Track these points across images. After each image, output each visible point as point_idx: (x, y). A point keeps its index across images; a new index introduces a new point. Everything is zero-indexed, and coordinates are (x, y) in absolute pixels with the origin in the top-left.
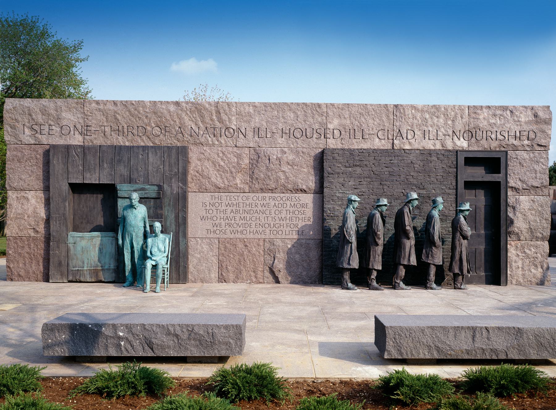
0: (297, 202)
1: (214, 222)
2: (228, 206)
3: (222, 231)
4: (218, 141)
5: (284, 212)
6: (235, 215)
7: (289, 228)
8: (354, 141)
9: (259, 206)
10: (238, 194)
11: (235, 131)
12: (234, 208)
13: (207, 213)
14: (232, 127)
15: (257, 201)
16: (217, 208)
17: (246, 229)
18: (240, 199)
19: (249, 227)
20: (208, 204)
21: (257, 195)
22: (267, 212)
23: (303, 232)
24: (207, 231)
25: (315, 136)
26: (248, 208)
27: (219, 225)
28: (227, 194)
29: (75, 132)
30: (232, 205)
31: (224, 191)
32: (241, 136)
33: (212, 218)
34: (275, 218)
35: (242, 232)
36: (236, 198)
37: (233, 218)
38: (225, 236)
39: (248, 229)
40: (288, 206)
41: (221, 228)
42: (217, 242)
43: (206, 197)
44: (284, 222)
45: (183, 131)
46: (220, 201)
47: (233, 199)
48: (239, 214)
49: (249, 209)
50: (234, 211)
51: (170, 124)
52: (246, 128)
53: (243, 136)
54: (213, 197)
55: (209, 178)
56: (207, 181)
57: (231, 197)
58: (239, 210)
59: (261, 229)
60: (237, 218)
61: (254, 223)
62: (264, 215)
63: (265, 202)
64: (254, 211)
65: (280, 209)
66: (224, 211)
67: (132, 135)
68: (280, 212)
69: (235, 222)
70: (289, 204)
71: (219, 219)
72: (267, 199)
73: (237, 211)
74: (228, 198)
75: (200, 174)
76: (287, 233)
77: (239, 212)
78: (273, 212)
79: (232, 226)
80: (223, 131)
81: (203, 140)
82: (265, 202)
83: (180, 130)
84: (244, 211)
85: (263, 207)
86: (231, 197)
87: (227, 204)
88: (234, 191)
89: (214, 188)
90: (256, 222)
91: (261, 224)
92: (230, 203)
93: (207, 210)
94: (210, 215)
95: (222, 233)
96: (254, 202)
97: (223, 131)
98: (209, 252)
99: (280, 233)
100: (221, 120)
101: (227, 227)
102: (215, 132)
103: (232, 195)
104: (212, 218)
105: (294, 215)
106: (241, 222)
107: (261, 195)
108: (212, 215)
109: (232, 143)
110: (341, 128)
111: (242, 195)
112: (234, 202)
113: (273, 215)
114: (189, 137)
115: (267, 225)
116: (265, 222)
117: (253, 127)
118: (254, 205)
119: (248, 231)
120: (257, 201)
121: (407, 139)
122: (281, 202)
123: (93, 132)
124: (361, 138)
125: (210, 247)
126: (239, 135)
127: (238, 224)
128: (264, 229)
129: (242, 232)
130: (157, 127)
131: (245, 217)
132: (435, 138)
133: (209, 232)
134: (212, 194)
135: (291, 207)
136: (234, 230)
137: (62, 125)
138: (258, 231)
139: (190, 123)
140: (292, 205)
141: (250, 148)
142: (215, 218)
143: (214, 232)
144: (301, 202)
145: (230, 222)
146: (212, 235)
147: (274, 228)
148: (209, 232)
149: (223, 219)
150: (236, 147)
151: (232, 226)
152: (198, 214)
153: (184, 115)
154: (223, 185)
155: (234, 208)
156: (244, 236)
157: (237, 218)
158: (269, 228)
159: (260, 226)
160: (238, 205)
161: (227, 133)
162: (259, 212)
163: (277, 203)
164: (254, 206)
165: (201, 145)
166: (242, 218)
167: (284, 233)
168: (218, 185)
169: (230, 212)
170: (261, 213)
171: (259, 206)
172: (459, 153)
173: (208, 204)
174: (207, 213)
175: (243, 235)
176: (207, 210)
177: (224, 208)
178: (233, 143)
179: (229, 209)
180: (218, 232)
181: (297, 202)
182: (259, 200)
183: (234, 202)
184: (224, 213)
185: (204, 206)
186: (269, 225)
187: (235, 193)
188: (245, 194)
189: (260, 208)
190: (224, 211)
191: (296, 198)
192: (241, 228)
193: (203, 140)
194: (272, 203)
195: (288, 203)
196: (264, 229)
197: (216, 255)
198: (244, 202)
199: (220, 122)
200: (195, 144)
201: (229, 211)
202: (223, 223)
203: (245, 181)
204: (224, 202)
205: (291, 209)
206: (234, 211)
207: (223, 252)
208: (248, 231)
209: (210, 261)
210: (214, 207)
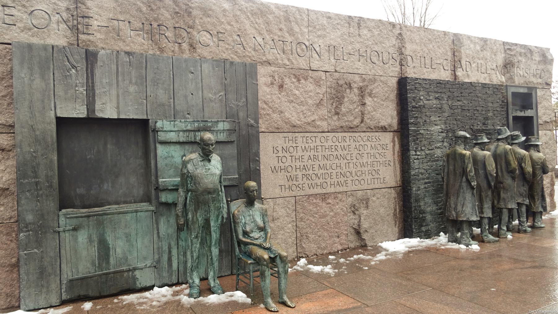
0: (377, 143)
1: (288, 175)
2: (305, 151)
3: (299, 186)
4: (289, 60)
5: (366, 155)
6: (313, 163)
7: (371, 176)
8: (425, 70)
9: (339, 150)
10: (315, 134)
11: (308, 48)
12: (312, 153)
13: (280, 161)
14: (305, 42)
15: (337, 143)
16: (292, 154)
17: (326, 181)
18: (318, 140)
19: (329, 179)
20: (280, 149)
21: (337, 135)
22: (348, 157)
23: (385, 179)
24: (280, 188)
25: (391, 62)
26: (328, 153)
27: (295, 179)
28: (302, 134)
29: (60, 24)
30: (309, 150)
31: (300, 130)
32: (315, 55)
33: (286, 169)
34: (357, 164)
35: (321, 186)
36: (313, 139)
37: (311, 168)
38: (303, 193)
39: (328, 180)
40: (369, 148)
41: (298, 182)
42: (293, 201)
43: (279, 141)
44: (366, 169)
45: (243, 42)
46: (294, 145)
47: (310, 141)
48: (317, 161)
49: (329, 153)
50: (312, 157)
51: (226, 30)
52: (320, 46)
53: (317, 56)
54: (287, 139)
55: (282, 112)
56: (278, 116)
57: (307, 139)
58: (317, 156)
59: (342, 179)
60: (316, 167)
61: (334, 172)
62: (345, 161)
63: (346, 144)
64: (335, 157)
65: (360, 153)
66: (301, 159)
67: (167, 41)
68: (361, 156)
69: (314, 172)
70: (369, 146)
71: (294, 170)
72: (347, 140)
73: (315, 158)
74: (305, 139)
75: (270, 107)
76: (369, 182)
77: (317, 158)
78: (354, 155)
79: (310, 178)
80: (294, 47)
81: (270, 57)
82: (346, 144)
83: (239, 39)
84: (323, 156)
85: (344, 150)
86: (307, 139)
87: (303, 148)
88: (312, 129)
89: (288, 126)
90: (337, 171)
91: (343, 173)
92: (307, 147)
93: (280, 158)
94: (284, 165)
95: (299, 189)
96: (334, 144)
97: (294, 47)
98: (286, 218)
99: (362, 182)
100: (291, 32)
101: (305, 179)
102: (285, 48)
103: (308, 136)
104: (286, 169)
105: (375, 160)
106: (321, 171)
107: (340, 135)
108: (287, 165)
109: (305, 65)
110: (413, 55)
111: (320, 134)
112: (311, 145)
113: (355, 160)
114: (253, 53)
115: (348, 174)
116: (347, 170)
117: (328, 45)
118: (334, 149)
119: (329, 183)
120: (337, 143)
121: (466, 71)
122: (362, 143)
123: (96, 28)
124: (430, 68)
125: (286, 210)
126: (313, 54)
127: (317, 175)
128: (346, 179)
129: (321, 186)
130: (205, 32)
131: (325, 165)
132: (485, 72)
133: (283, 189)
134: (285, 135)
135: (372, 150)
136: (313, 182)
137: (33, 9)
138: (340, 183)
139: (254, 31)
140: (373, 146)
141: (326, 72)
142: (290, 169)
143: (290, 188)
144: (381, 143)
145: (307, 173)
146: (287, 193)
147: (356, 178)
148: (283, 189)
149: (299, 170)
150: (310, 70)
151: (310, 178)
152: (267, 164)
153: (243, 17)
154: (299, 123)
155: (312, 153)
156: (324, 191)
157: (316, 167)
158: (351, 177)
159: (342, 176)
160: (316, 148)
161: (298, 50)
162: (339, 158)
163: (358, 144)
164: (333, 150)
165: (267, 65)
166: (322, 166)
167: (366, 183)
168: (293, 122)
169: (307, 159)
170: (342, 159)
171: (339, 150)
172: (508, 87)
173: (280, 149)
174: (280, 161)
175: (324, 190)
176: (280, 158)
177: (300, 153)
178: (306, 64)
179: (307, 155)
180: (294, 188)
181: (377, 143)
182: (340, 141)
183: (311, 145)
184: (301, 161)
185: (275, 151)
186: (351, 173)
187: (312, 133)
188: (324, 134)
189: (340, 152)
190: (301, 159)
191: (377, 138)
192: (321, 180)
193: (271, 58)
194: (353, 145)
195: (368, 143)
196: (346, 179)
197: (293, 221)
198: (322, 144)
199: (290, 34)
200: (262, 63)
201: (306, 158)
202: (300, 174)
203: (323, 117)
204: (300, 147)
205: (372, 152)
206: (312, 157)
207: (302, 215)
208: (329, 183)
209: (288, 231)
210: (288, 152)
